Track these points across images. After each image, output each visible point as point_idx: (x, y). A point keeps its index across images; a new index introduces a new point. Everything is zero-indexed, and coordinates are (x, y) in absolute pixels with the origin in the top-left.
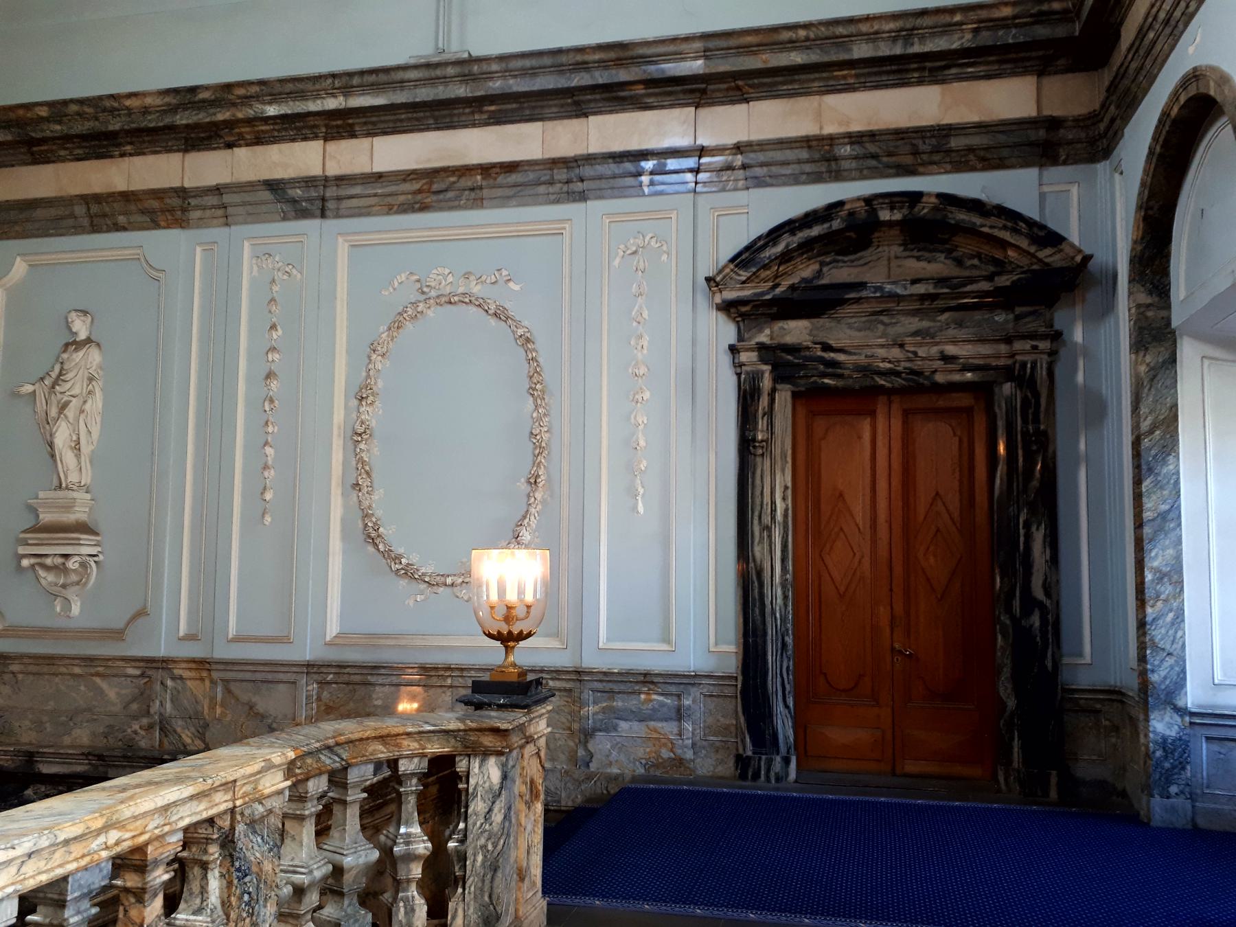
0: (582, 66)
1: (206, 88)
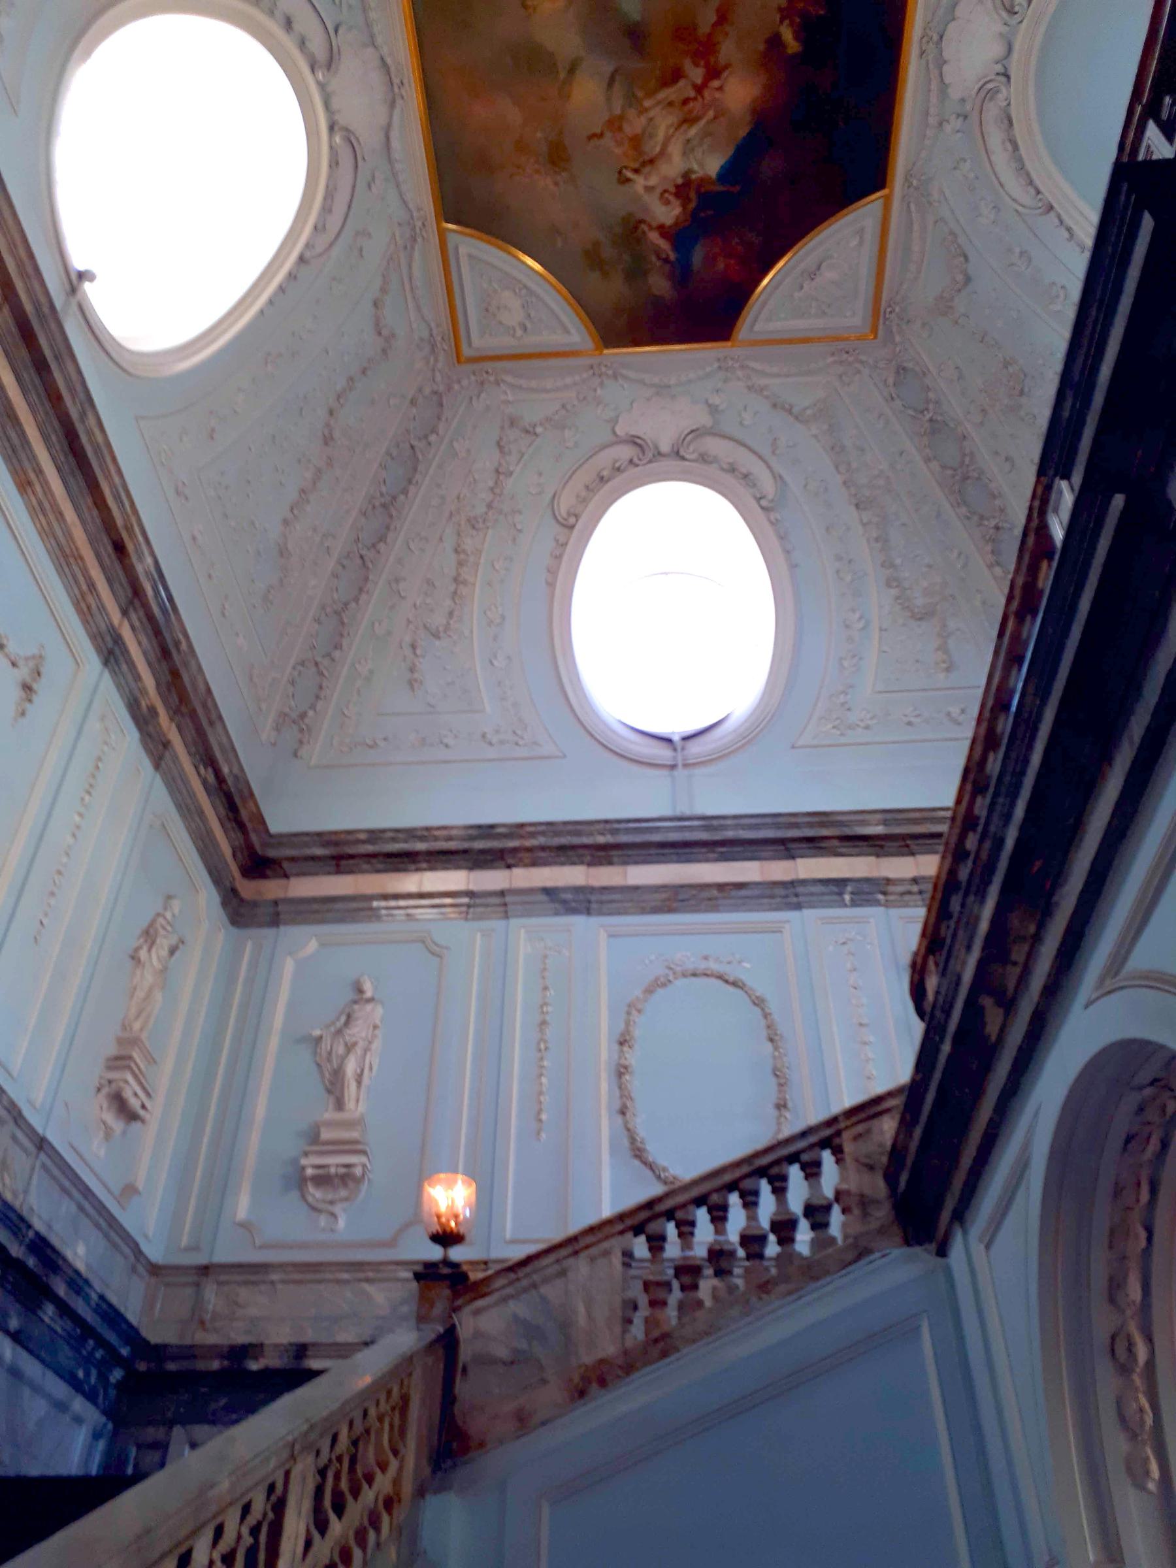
0: (796, 826)
1: (504, 825)
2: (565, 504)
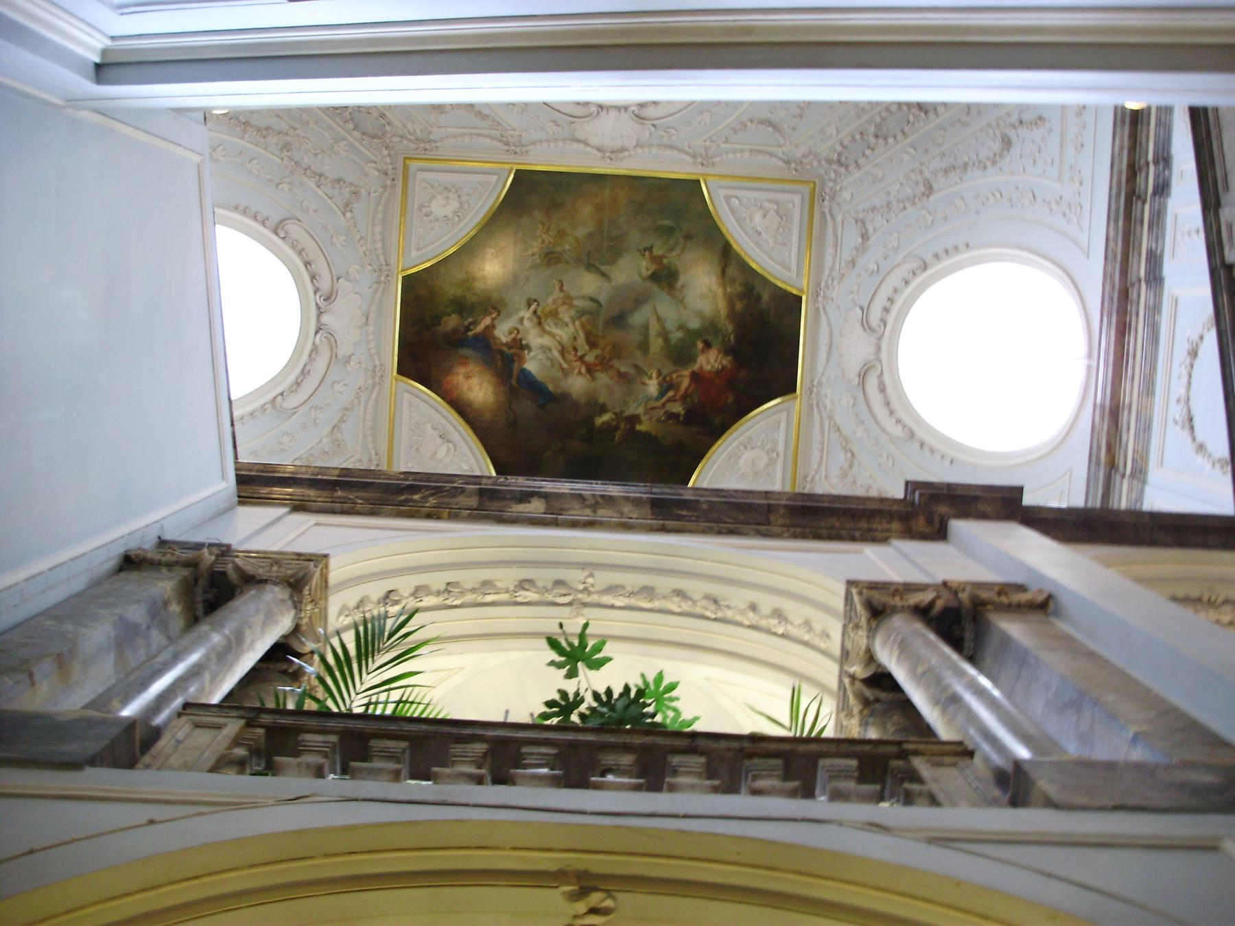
2: (292, 227)
